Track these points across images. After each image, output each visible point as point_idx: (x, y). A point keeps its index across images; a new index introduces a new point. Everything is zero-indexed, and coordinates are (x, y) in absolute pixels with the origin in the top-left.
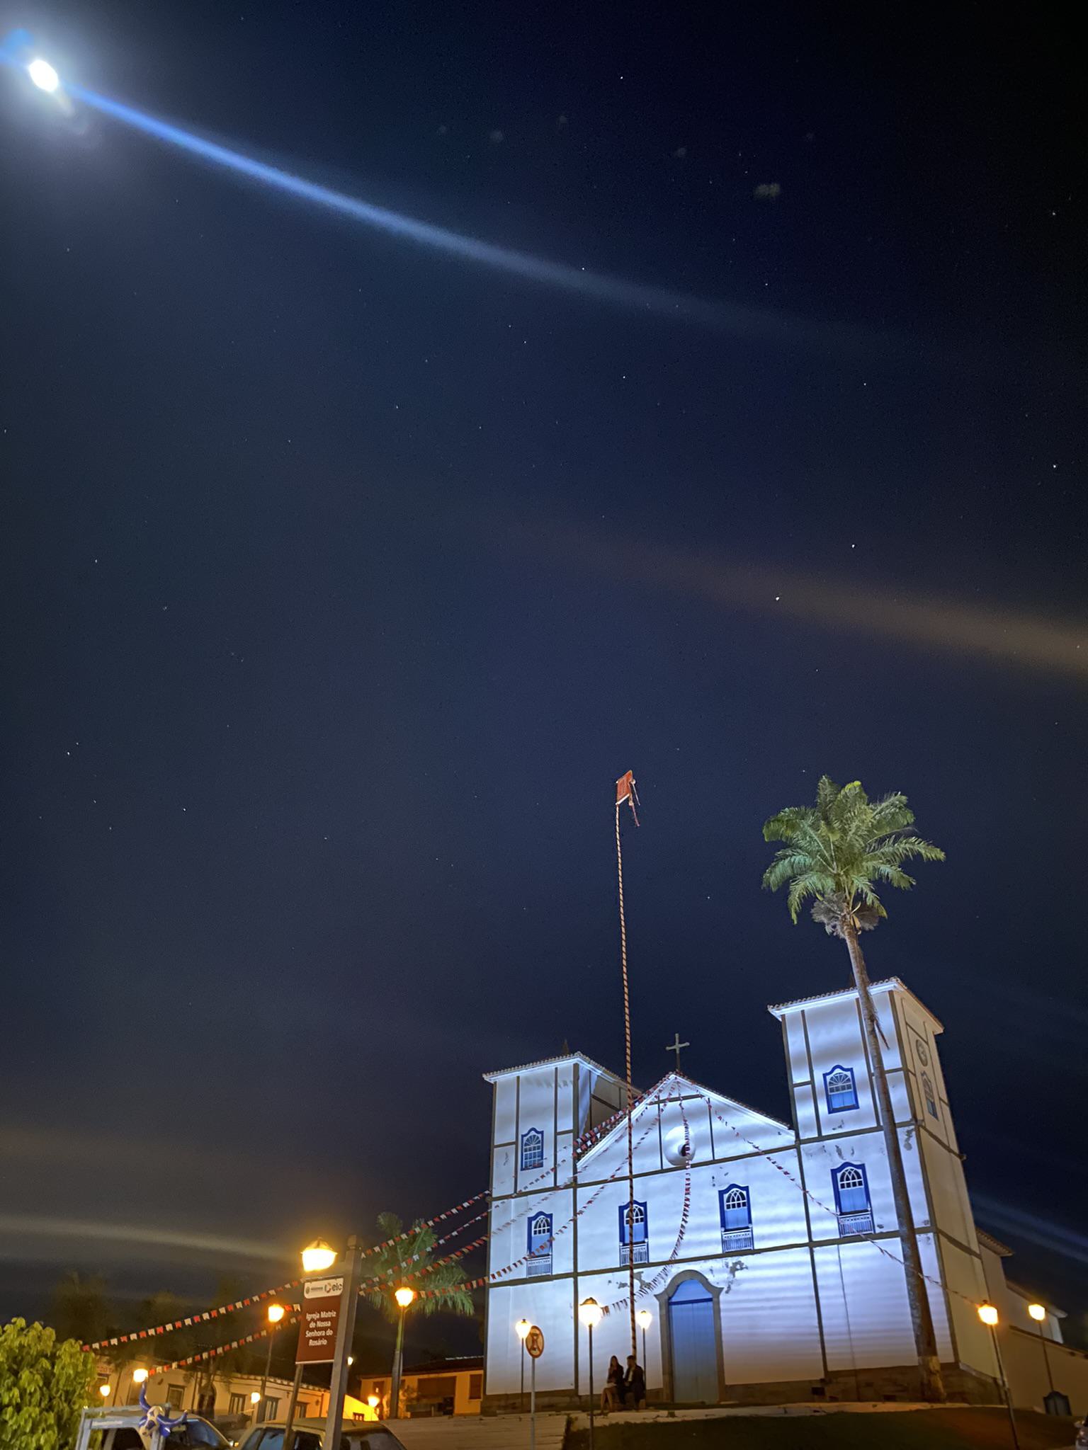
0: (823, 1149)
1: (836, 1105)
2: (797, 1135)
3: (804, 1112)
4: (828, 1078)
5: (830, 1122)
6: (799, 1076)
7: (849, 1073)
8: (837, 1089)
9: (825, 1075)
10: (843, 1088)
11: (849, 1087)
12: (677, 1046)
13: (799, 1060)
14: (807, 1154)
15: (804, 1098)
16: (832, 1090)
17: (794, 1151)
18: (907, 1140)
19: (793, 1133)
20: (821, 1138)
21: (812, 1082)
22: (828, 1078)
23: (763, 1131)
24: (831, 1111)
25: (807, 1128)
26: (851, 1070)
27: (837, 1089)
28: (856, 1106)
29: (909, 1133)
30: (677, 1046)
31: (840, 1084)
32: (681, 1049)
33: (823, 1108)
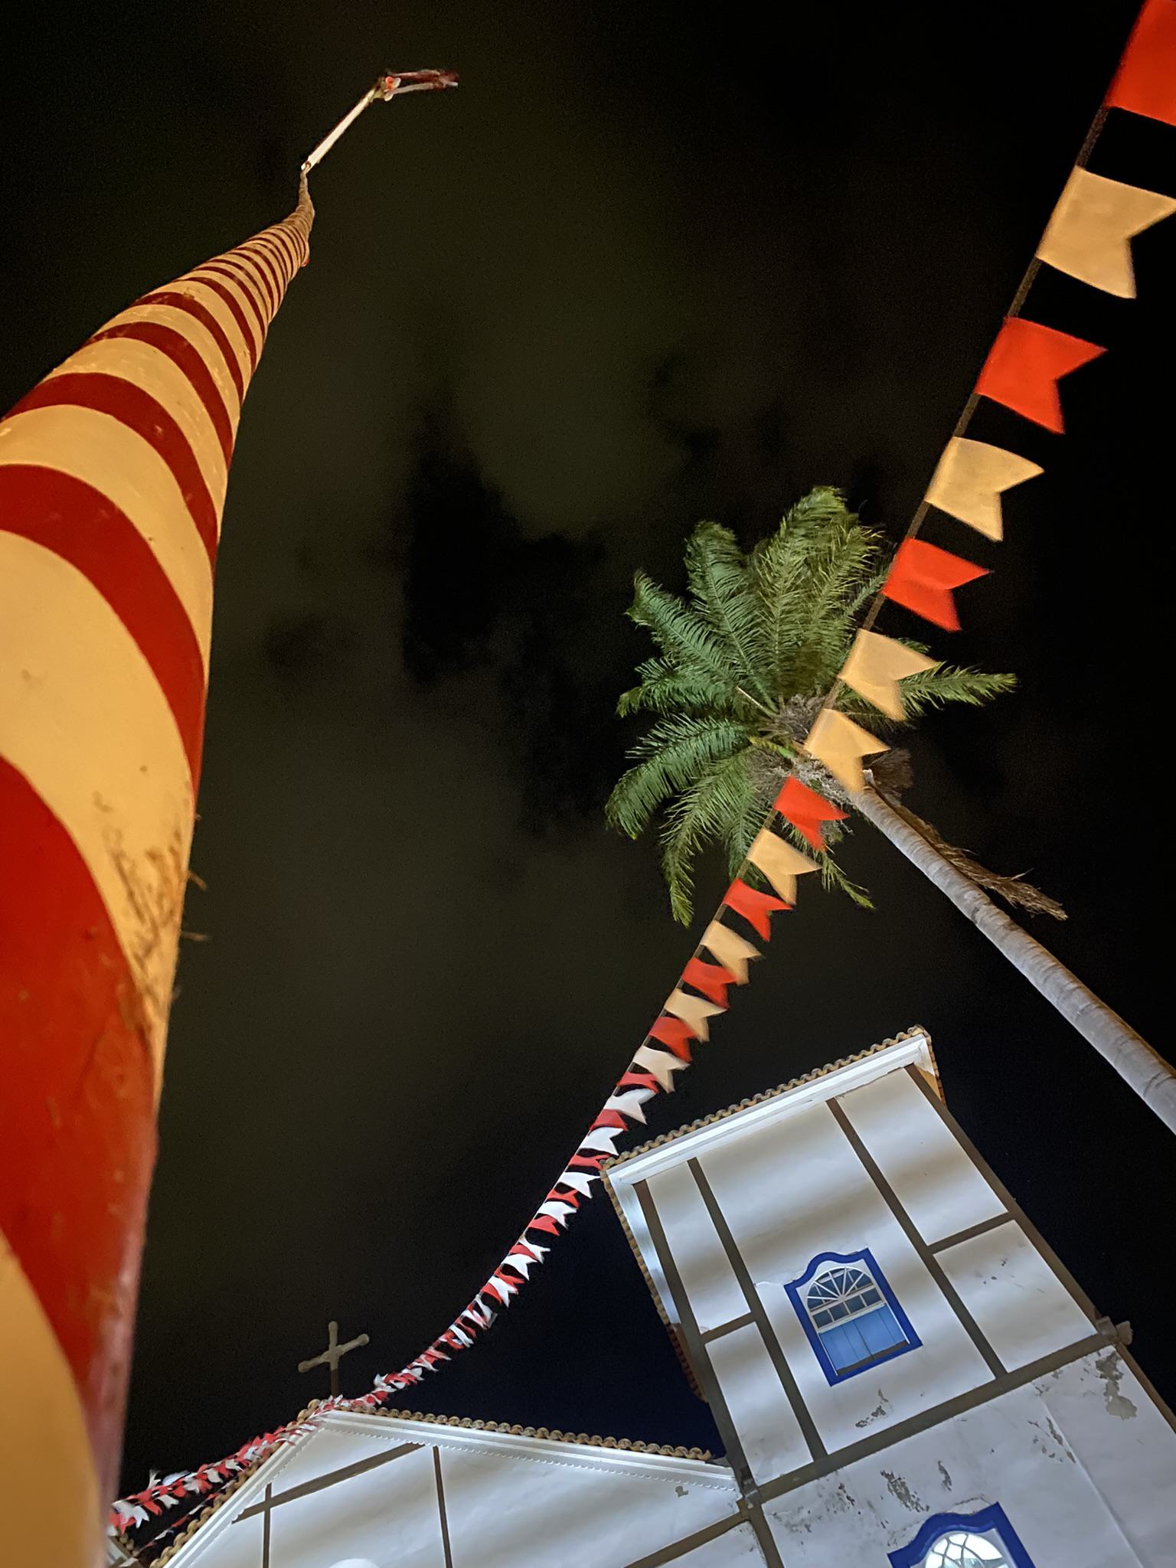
0: (843, 1497)
1: (845, 1353)
2: (744, 1476)
3: (749, 1398)
4: (803, 1291)
5: (839, 1410)
6: (715, 1309)
7: (860, 1266)
8: (839, 1312)
9: (791, 1289)
10: (856, 1305)
11: (872, 1298)
12: (333, 1354)
13: (705, 1270)
14: (791, 1527)
15: (741, 1357)
16: (823, 1320)
17: (744, 1533)
18: (1112, 1389)
19: (726, 1475)
20: (824, 1464)
21: (757, 1313)
22: (803, 1291)
23: (621, 1497)
24: (833, 1378)
25: (771, 1442)
26: (866, 1255)
27: (839, 1312)
28: (916, 1343)
29: (1106, 1368)
30: (333, 1354)
31: (842, 1299)
32: (343, 1359)
33: (807, 1370)
